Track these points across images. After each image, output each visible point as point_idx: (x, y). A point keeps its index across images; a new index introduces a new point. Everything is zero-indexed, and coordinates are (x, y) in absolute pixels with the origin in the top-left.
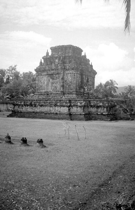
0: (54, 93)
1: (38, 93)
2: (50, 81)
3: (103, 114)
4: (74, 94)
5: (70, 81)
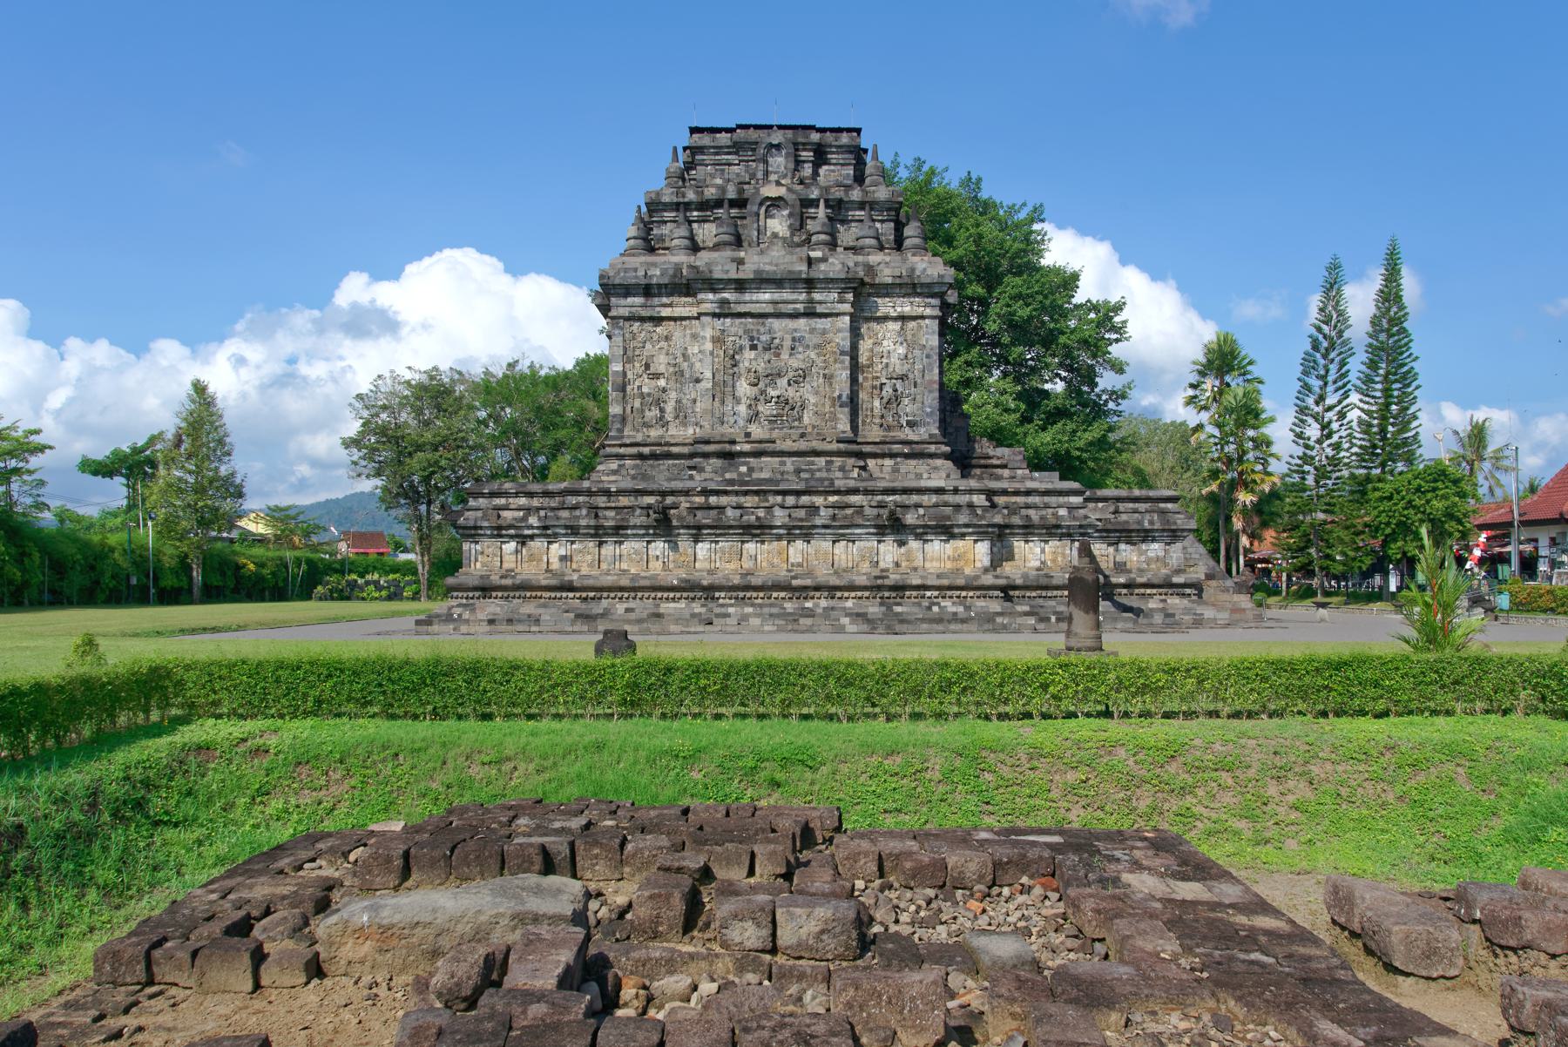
3: (1176, 580)
4: (932, 456)
5: (899, 370)
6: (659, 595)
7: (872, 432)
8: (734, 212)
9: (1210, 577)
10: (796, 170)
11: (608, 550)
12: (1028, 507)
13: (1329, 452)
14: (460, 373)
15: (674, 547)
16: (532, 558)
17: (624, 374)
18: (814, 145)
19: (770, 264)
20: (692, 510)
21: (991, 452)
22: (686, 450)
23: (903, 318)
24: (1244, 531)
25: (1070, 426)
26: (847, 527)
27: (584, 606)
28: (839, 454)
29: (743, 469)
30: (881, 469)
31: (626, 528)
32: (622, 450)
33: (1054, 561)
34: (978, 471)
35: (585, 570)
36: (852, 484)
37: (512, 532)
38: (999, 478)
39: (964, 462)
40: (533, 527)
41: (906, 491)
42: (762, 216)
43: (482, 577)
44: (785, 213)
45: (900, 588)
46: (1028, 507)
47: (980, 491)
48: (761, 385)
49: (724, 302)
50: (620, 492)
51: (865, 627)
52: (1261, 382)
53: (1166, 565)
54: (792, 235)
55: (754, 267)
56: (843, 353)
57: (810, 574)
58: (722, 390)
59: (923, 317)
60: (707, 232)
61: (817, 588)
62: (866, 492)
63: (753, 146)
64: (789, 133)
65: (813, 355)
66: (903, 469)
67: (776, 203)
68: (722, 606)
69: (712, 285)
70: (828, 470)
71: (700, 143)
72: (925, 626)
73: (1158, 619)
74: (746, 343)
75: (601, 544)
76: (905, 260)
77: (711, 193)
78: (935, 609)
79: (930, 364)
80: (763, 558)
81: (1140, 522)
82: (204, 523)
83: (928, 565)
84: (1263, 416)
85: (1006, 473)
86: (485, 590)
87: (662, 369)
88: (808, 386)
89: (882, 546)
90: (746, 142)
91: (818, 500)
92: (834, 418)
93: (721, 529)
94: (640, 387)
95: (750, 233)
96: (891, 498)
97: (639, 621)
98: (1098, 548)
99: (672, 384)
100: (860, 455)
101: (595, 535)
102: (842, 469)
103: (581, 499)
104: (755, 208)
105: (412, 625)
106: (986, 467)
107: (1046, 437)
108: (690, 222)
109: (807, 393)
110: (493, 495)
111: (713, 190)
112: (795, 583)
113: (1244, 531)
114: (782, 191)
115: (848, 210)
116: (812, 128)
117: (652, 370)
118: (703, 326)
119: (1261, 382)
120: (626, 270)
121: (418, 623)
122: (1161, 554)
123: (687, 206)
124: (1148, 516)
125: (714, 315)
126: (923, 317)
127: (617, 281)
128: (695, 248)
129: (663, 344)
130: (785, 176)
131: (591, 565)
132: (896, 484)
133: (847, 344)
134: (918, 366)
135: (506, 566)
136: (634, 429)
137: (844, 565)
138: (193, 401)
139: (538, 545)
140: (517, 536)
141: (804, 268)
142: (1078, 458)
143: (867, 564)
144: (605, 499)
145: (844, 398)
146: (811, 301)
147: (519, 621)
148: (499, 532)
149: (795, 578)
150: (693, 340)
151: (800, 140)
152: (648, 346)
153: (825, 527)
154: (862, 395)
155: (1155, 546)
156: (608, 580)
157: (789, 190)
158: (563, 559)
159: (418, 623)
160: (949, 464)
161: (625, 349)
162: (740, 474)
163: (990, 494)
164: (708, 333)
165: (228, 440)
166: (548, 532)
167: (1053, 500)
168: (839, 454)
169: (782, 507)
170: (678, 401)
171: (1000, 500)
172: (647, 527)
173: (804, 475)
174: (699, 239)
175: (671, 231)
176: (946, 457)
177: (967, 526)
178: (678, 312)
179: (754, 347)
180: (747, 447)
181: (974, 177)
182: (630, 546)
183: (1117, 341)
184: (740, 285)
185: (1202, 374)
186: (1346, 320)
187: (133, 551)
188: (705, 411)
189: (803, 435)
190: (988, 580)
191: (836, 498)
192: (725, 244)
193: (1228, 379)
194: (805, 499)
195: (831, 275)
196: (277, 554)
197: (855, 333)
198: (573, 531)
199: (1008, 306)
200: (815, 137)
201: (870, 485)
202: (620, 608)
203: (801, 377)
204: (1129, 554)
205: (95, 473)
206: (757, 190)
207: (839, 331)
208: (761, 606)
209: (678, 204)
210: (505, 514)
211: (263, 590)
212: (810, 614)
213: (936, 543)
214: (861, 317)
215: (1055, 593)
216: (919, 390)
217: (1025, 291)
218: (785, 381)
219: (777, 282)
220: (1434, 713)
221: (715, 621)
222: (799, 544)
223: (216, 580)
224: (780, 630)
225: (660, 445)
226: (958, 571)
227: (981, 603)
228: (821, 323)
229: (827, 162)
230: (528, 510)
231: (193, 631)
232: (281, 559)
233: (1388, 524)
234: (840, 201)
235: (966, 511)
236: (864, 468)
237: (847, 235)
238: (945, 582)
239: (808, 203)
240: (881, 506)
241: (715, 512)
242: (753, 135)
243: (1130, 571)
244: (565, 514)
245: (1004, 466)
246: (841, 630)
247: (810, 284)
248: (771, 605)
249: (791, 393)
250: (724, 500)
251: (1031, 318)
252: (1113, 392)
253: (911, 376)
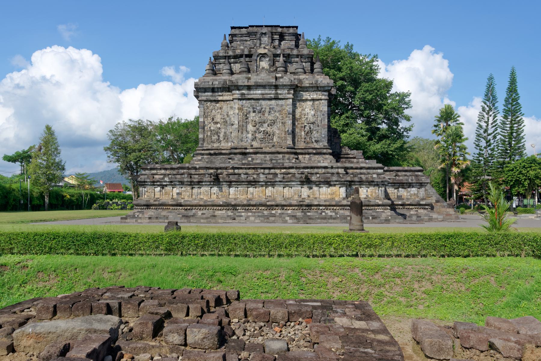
0: (264, 150)
1: (207, 152)
2: (251, 118)
3: (422, 203)
4: (324, 154)
5: (312, 120)
6: (215, 208)
7: (301, 145)
8: (247, 59)
9: (437, 201)
10: (272, 42)
11: (195, 190)
12: (361, 174)
13: (490, 152)
14: (150, 122)
15: (221, 190)
16: (166, 193)
17: (204, 122)
18: (279, 33)
19: (261, 79)
20: (228, 175)
21: (349, 152)
22: (227, 152)
23: (313, 100)
24: (456, 183)
25: (388, 142)
26: (289, 182)
27: (186, 212)
28: (288, 153)
29: (250, 159)
30: (305, 160)
31: (202, 182)
32: (203, 152)
33: (371, 195)
34: (344, 160)
35: (186, 198)
36: (291, 165)
37: (158, 183)
38: (352, 162)
39: (337, 156)
40: (166, 182)
41: (312, 168)
42: (258, 61)
43: (147, 201)
44: (267, 59)
45: (309, 206)
46: (361, 174)
47: (342, 168)
48: (257, 126)
49: (243, 94)
50: (200, 168)
51: (295, 221)
52: (463, 124)
53: (418, 197)
54: (270, 68)
55: (255, 81)
56: (289, 114)
57: (274, 200)
58: (242, 128)
59: (321, 100)
60: (236, 67)
61: (277, 206)
62: (297, 168)
63: (255, 33)
64: (270, 28)
65: (277, 115)
66: (313, 159)
67: (264, 55)
68: (240, 212)
69: (238, 88)
70: (283, 159)
71: (235, 33)
72: (319, 220)
73: (414, 218)
74: (251, 110)
75: (192, 188)
76: (314, 77)
77: (238, 52)
78: (323, 214)
79: (324, 118)
80: (256, 193)
81: (407, 180)
82: (49, 180)
83: (321, 196)
84: (463, 138)
85: (355, 160)
86: (148, 206)
87: (219, 120)
88: (275, 127)
89: (303, 189)
90: (252, 32)
91: (278, 171)
92: (286, 139)
93: (239, 183)
94: (210, 127)
95: (253, 67)
96: (306, 170)
97: (207, 218)
98: (391, 191)
99: (223, 126)
100: (296, 154)
101: (191, 185)
102: (288, 159)
103: (185, 171)
104: (255, 58)
105: (120, 220)
106: (347, 158)
107: (378, 146)
108: (230, 63)
109: (275, 129)
110: (151, 169)
111: (239, 51)
112: (268, 203)
113: (456, 183)
114: (266, 51)
115: (292, 58)
116: (278, 26)
117: (215, 121)
118: (235, 103)
119: (463, 124)
120: (205, 82)
121: (122, 218)
122: (416, 192)
123: (229, 57)
124: (410, 178)
125: (239, 99)
126: (321, 100)
127: (201, 87)
128: (232, 73)
129: (219, 110)
130: (268, 45)
131: (188, 196)
132: (309, 165)
133: (291, 110)
134: (319, 119)
135: (156, 196)
136: (208, 143)
137: (287, 196)
138: (46, 134)
139: (169, 188)
140: (160, 185)
141: (274, 81)
142: (391, 154)
143: (297, 196)
144: (194, 171)
145: (290, 131)
146: (277, 94)
147: (160, 218)
148: (153, 183)
149: (268, 201)
150: (231, 109)
151: (274, 31)
152: (213, 111)
153: (280, 182)
154: (297, 130)
155: (414, 189)
156: (195, 202)
157: (269, 50)
158: (178, 194)
159: (122, 218)
160: (331, 157)
161: (204, 113)
162: (249, 161)
163: (346, 169)
164: (237, 106)
165: (59, 148)
166: (172, 184)
167: (371, 171)
168: (288, 153)
169: (264, 174)
170: (225, 133)
171: (350, 171)
172: (210, 182)
173: (273, 161)
174: (234, 70)
175: (223, 67)
176: (330, 154)
177: (336, 181)
178: (225, 98)
179: (254, 112)
180: (251, 151)
181: (350, 44)
182: (204, 189)
183: (407, 108)
184: (249, 88)
185: (439, 121)
186: (496, 99)
187: (22, 191)
188: (235, 137)
189: (273, 146)
190: (345, 202)
191: (285, 170)
192: (244, 72)
193: (449, 123)
194: (272, 171)
195: (285, 84)
196: (79, 191)
197: (294, 106)
198: (182, 183)
199: (363, 95)
200: (280, 30)
201: (298, 165)
202: (200, 213)
203: (273, 123)
204: (403, 192)
205: (9, 161)
206: (256, 51)
207: (288, 105)
208: (255, 212)
209: (225, 56)
210: (156, 176)
211: (73, 206)
212: (274, 216)
213: (324, 188)
214: (296, 100)
215: (372, 208)
216: (319, 128)
217: (370, 89)
218: (266, 125)
219: (263, 87)
220: (488, 256)
221: (236, 218)
222: (270, 188)
223: (54, 202)
224: (262, 222)
225: (218, 150)
226: (333, 199)
227: (341, 212)
228: (280, 102)
229: (284, 40)
230: (165, 175)
231: (36, 221)
232: (80, 193)
233: (511, 181)
234: (289, 55)
235: (336, 175)
236: (297, 159)
237: (291, 68)
238: (328, 203)
239: (276, 56)
240: (302, 173)
241: (236, 176)
242: (255, 29)
243: (403, 199)
244: (178, 176)
245: (355, 158)
246: (286, 222)
247: (276, 87)
248: (259, 212)
249: (269, 129)
250: (241, 171)
251: (372, 99)
252: (406, 128)
253: (316, 123)
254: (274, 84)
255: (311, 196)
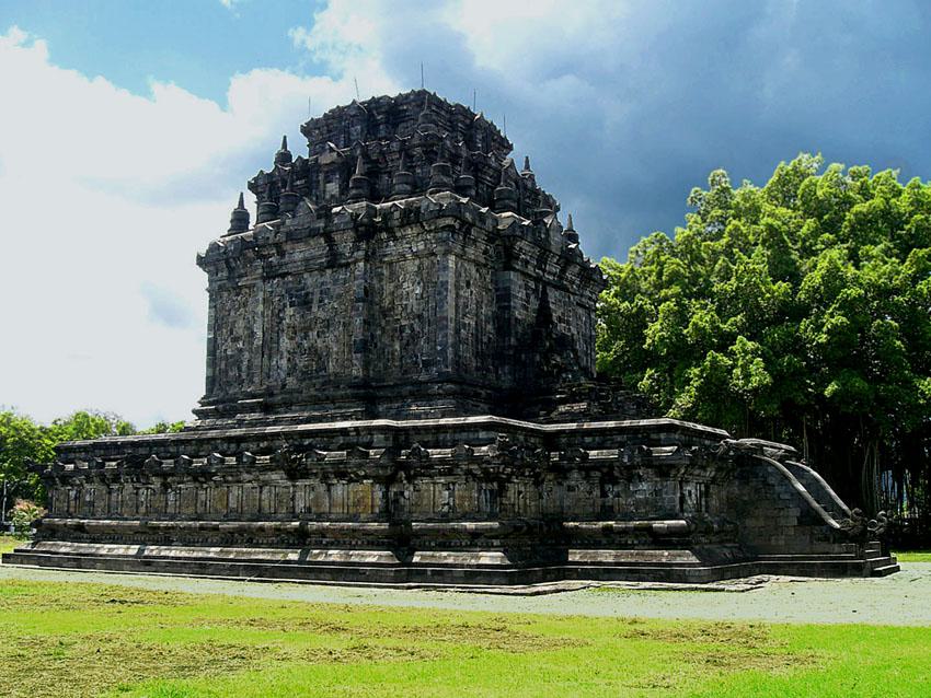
56: (358, 300)
87: (241, 332)
152: (232, 313)
155: (644, 486)
254: (322, 231)
255: (313, 509)
